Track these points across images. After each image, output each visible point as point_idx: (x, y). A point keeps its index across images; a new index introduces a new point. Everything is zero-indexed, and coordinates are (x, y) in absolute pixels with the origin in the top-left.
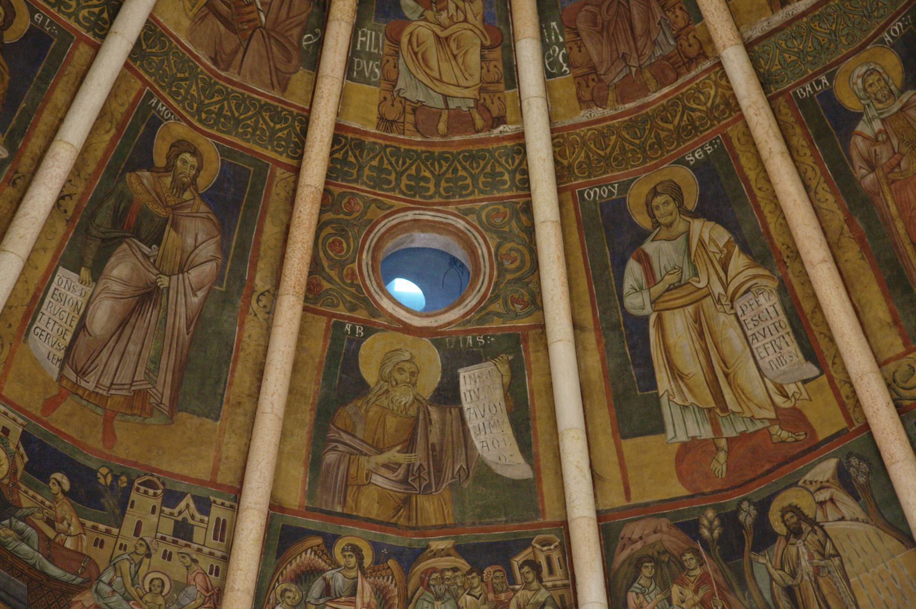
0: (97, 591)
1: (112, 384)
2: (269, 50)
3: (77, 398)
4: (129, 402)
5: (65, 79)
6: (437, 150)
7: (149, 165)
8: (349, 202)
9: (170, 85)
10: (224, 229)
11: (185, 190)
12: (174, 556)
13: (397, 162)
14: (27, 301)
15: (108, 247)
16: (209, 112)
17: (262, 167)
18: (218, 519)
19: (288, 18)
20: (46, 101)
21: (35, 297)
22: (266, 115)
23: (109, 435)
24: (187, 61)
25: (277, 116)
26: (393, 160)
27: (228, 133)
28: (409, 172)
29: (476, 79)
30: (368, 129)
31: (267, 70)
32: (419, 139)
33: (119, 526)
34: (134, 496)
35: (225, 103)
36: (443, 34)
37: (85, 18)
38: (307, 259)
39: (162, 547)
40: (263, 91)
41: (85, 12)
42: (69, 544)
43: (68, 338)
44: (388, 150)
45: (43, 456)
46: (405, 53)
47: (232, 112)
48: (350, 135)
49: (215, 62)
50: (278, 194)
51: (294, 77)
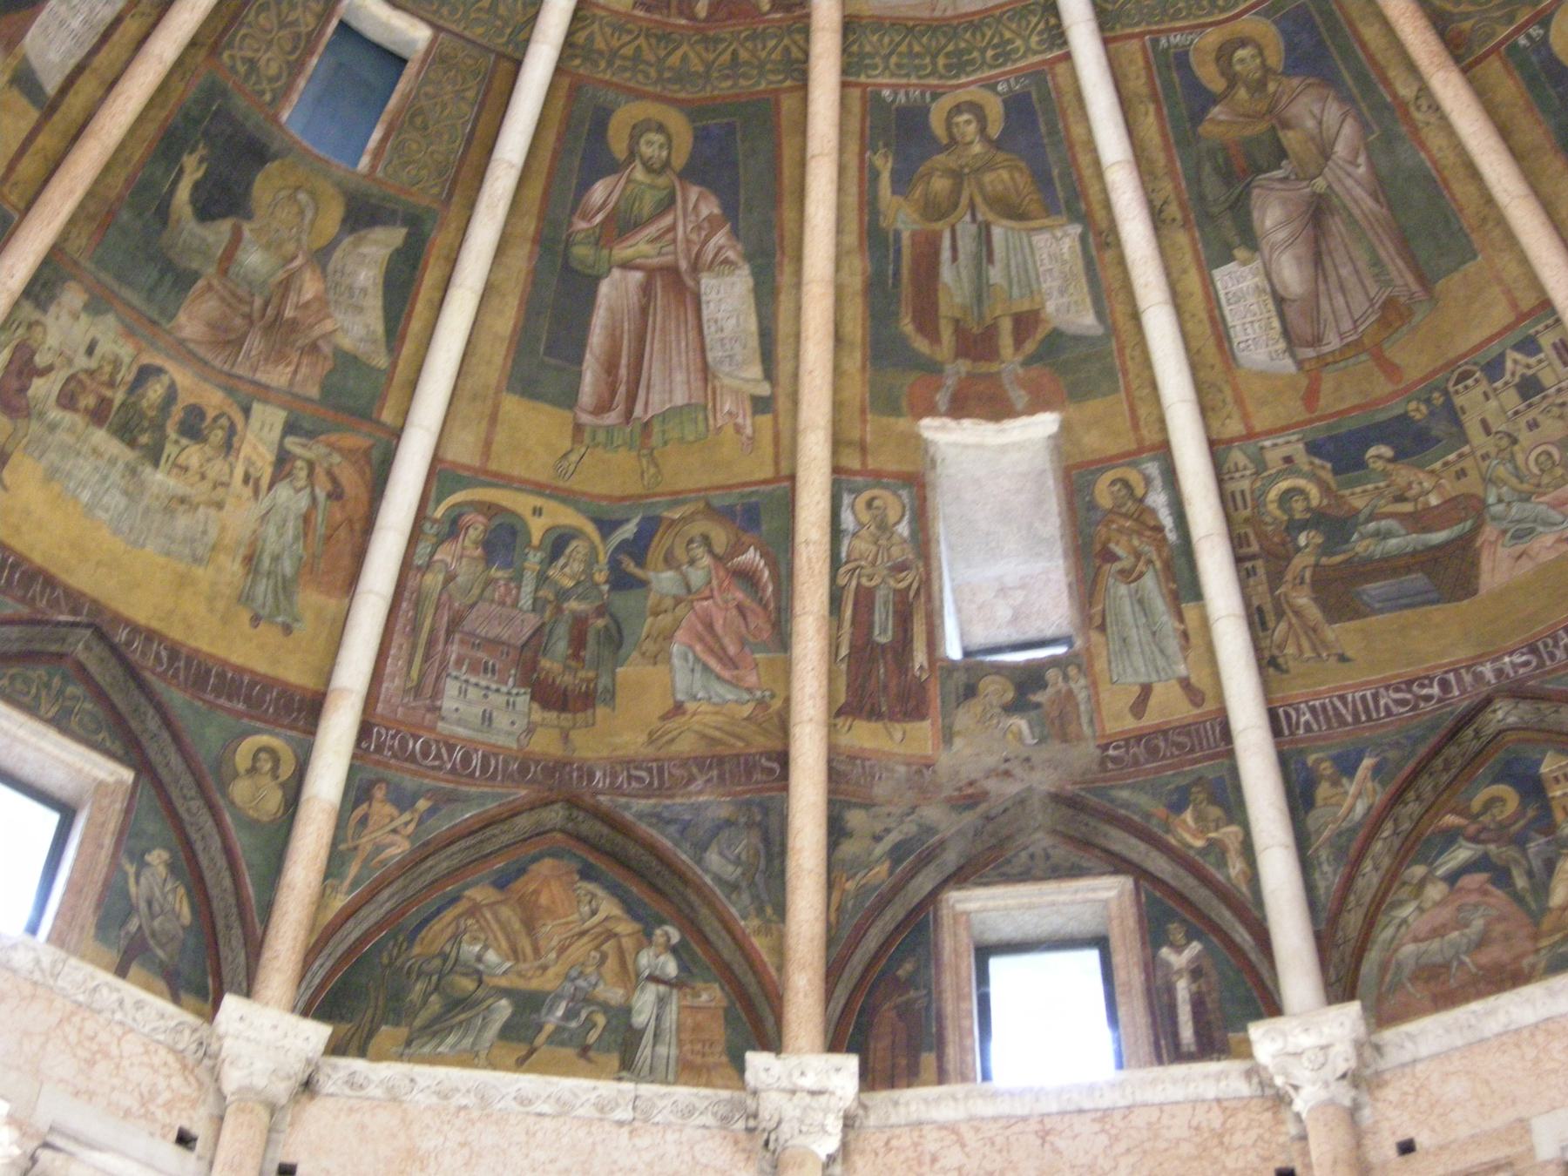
0: (1494, 518)
1: (1355, 322)
3: (1331, 367)
4: (1384, 322)
5: (1069, 111)
7: (1214, 100)
9: (1164, 12)
10: (1328, 80)
11: (1265, 85)
12: (1540, 418)
14: (1209, 331)
15: (1240, 210)
18: (1555, 346)
20: (1071, 147)
21: (1212, 320)
23: (1391, 370)
33: (1467, 442)
34: (1459, 401)
37: (1040, 42)
38: (1422, 23)
39: (1522, 422)
41: (1034, 39)
42: (1434, 500)
43: (1276, 323)
45: (1341, 451)
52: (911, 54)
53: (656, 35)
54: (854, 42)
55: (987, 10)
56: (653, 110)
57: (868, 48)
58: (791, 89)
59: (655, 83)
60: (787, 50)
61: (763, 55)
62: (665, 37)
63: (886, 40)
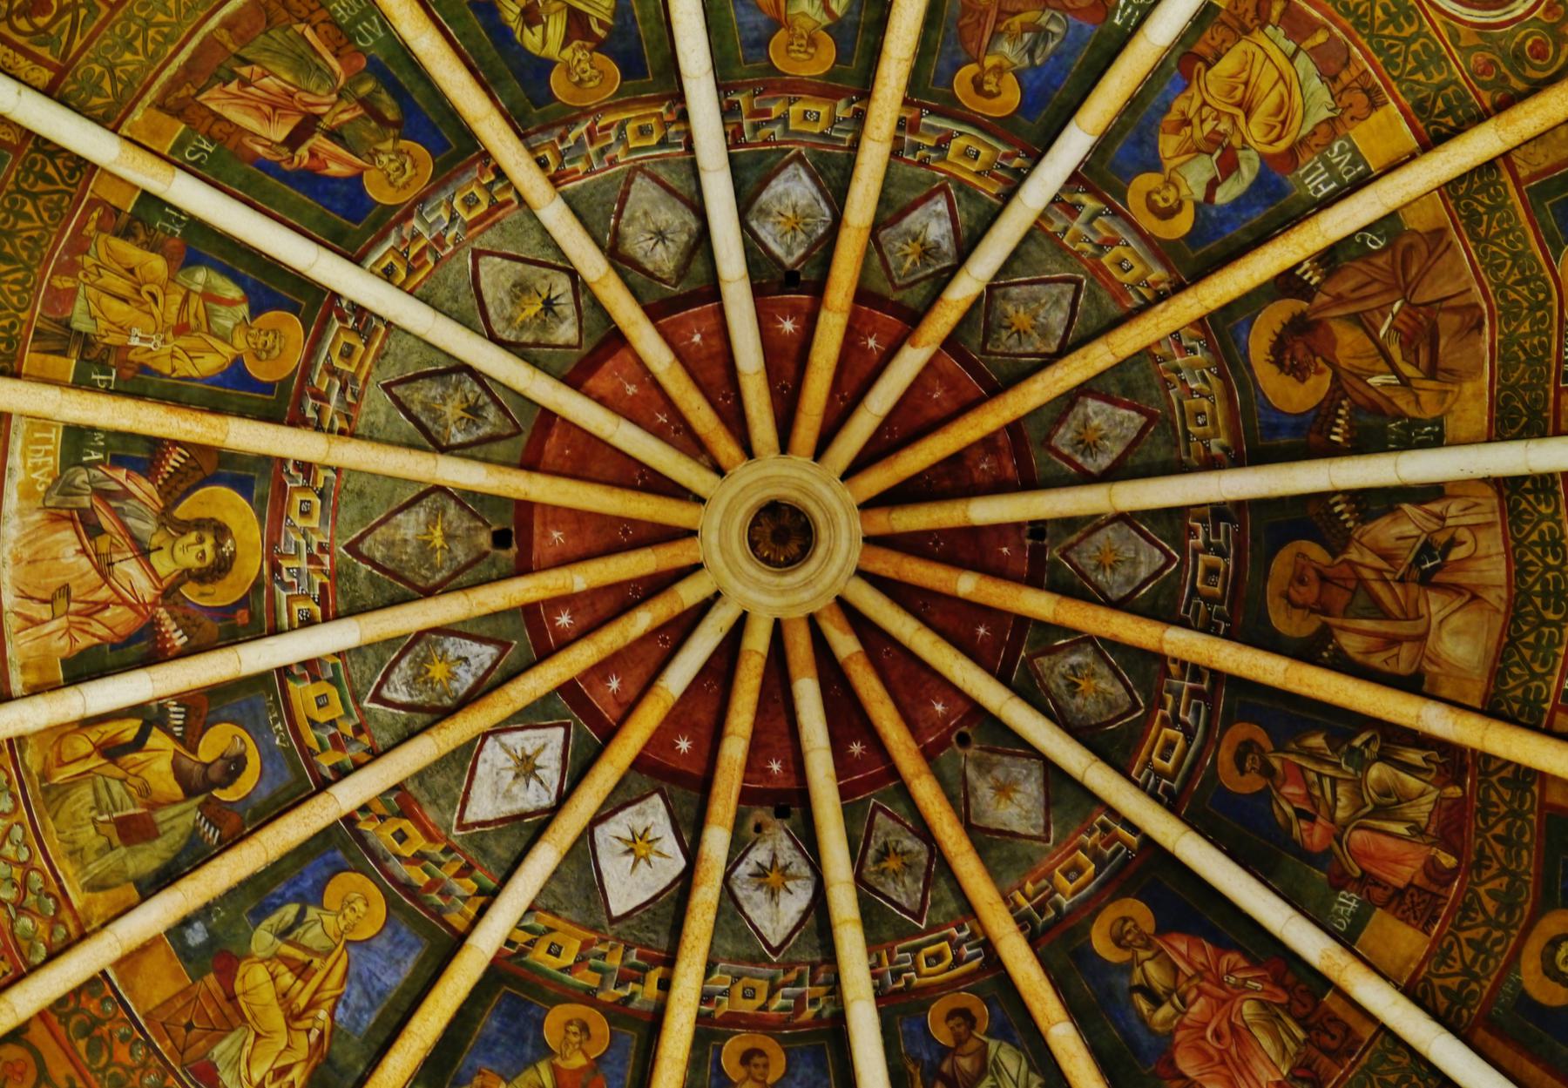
2: (1424, 272)
6: (1347, 22)
8: (1483, 73)
13: (1398, 54)
16: (1533, 293)
17: (1535, 197)
19: (1375, 280)
22: (1482, 230)
24: (1504, 360)
25: (1473, 220)
26: (1400, 60)
27: (1534, 256)
28: (1396, 33)
29: (1243, 45)
30: (1397, 111)
31: (1439, 263)
32: (1355, 49)
35: (1509, 282)
36: (1240, 113)
37: (1548, 506)
40: (1463, 253)
41: (1543, 508)
44: (1395, 74)
46: (1294, 134)
47: (1512, 268)
48: (1420, 125)
49: (1479, 326)
50: (1546, 156)
51: (1421, 229)
52: (1535, 647)
53: (1462, 919)
54: (1510, 708)
55: (1507, 552)
56: (1535, 945)
57: (1519, 692)
58: (1543, 789)
59: (1509, 936)
60: (1502, 781)
61: (1503, 809)
62: (1466, 908)
63: (1516, 670)
